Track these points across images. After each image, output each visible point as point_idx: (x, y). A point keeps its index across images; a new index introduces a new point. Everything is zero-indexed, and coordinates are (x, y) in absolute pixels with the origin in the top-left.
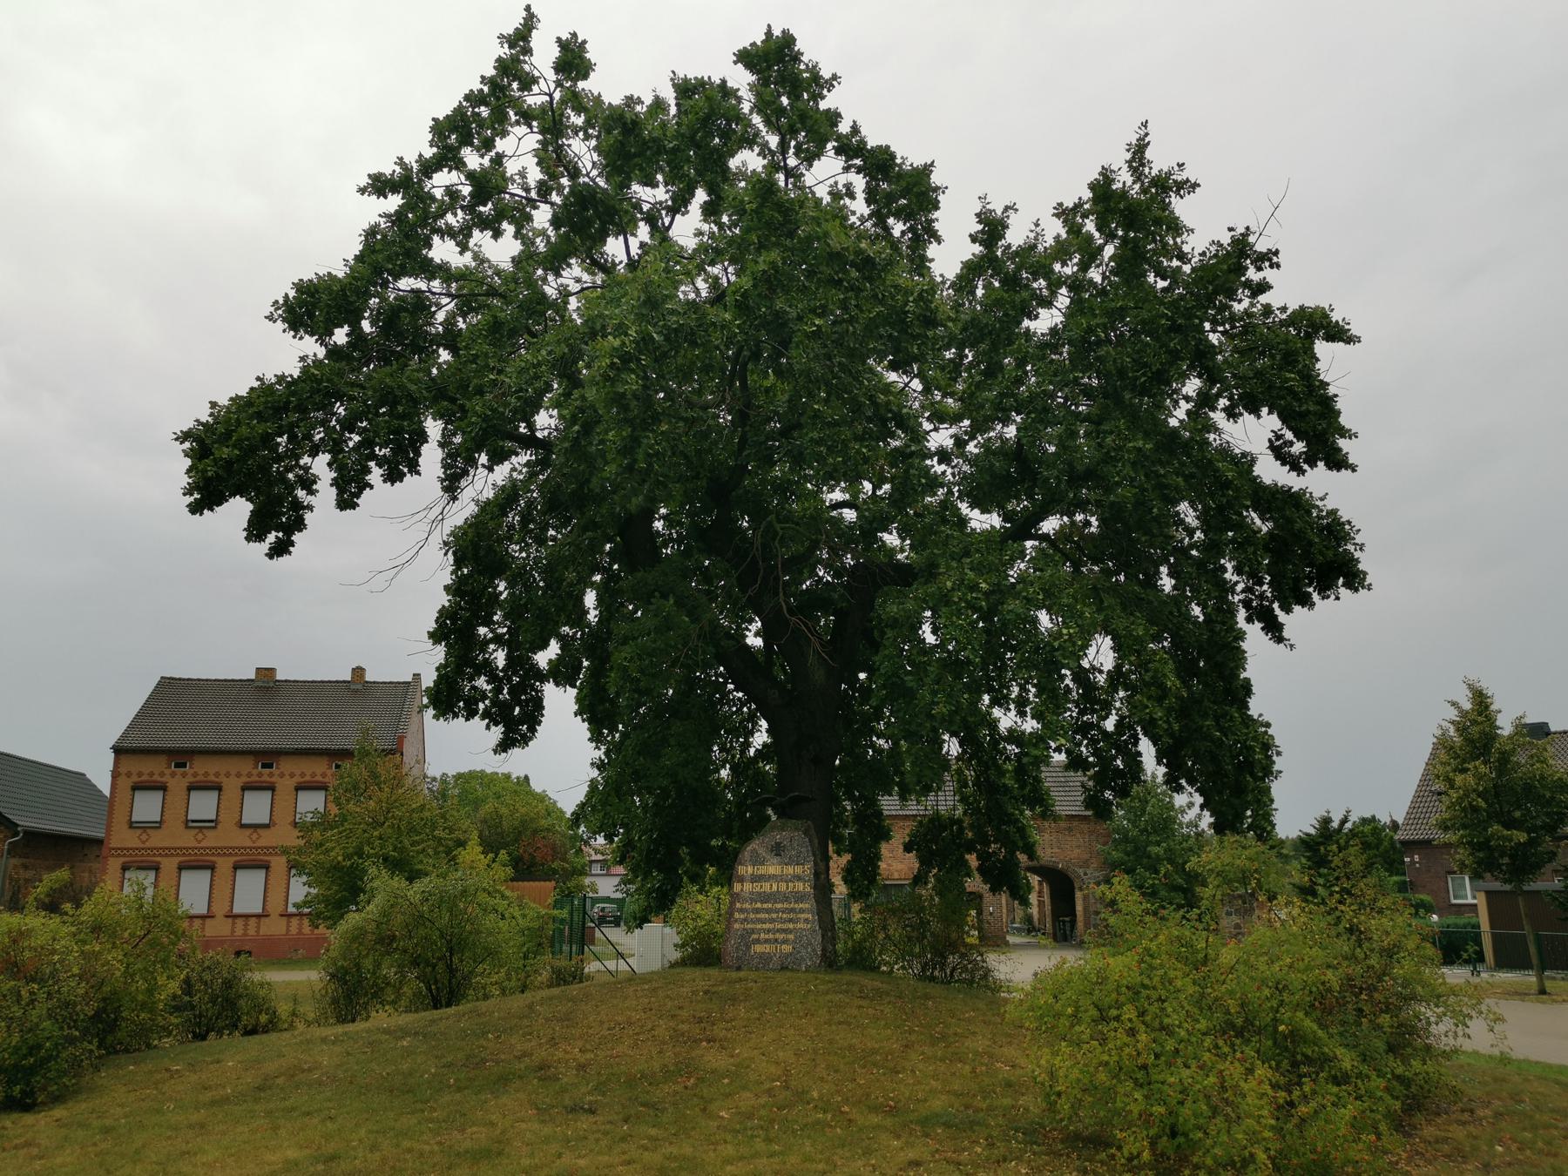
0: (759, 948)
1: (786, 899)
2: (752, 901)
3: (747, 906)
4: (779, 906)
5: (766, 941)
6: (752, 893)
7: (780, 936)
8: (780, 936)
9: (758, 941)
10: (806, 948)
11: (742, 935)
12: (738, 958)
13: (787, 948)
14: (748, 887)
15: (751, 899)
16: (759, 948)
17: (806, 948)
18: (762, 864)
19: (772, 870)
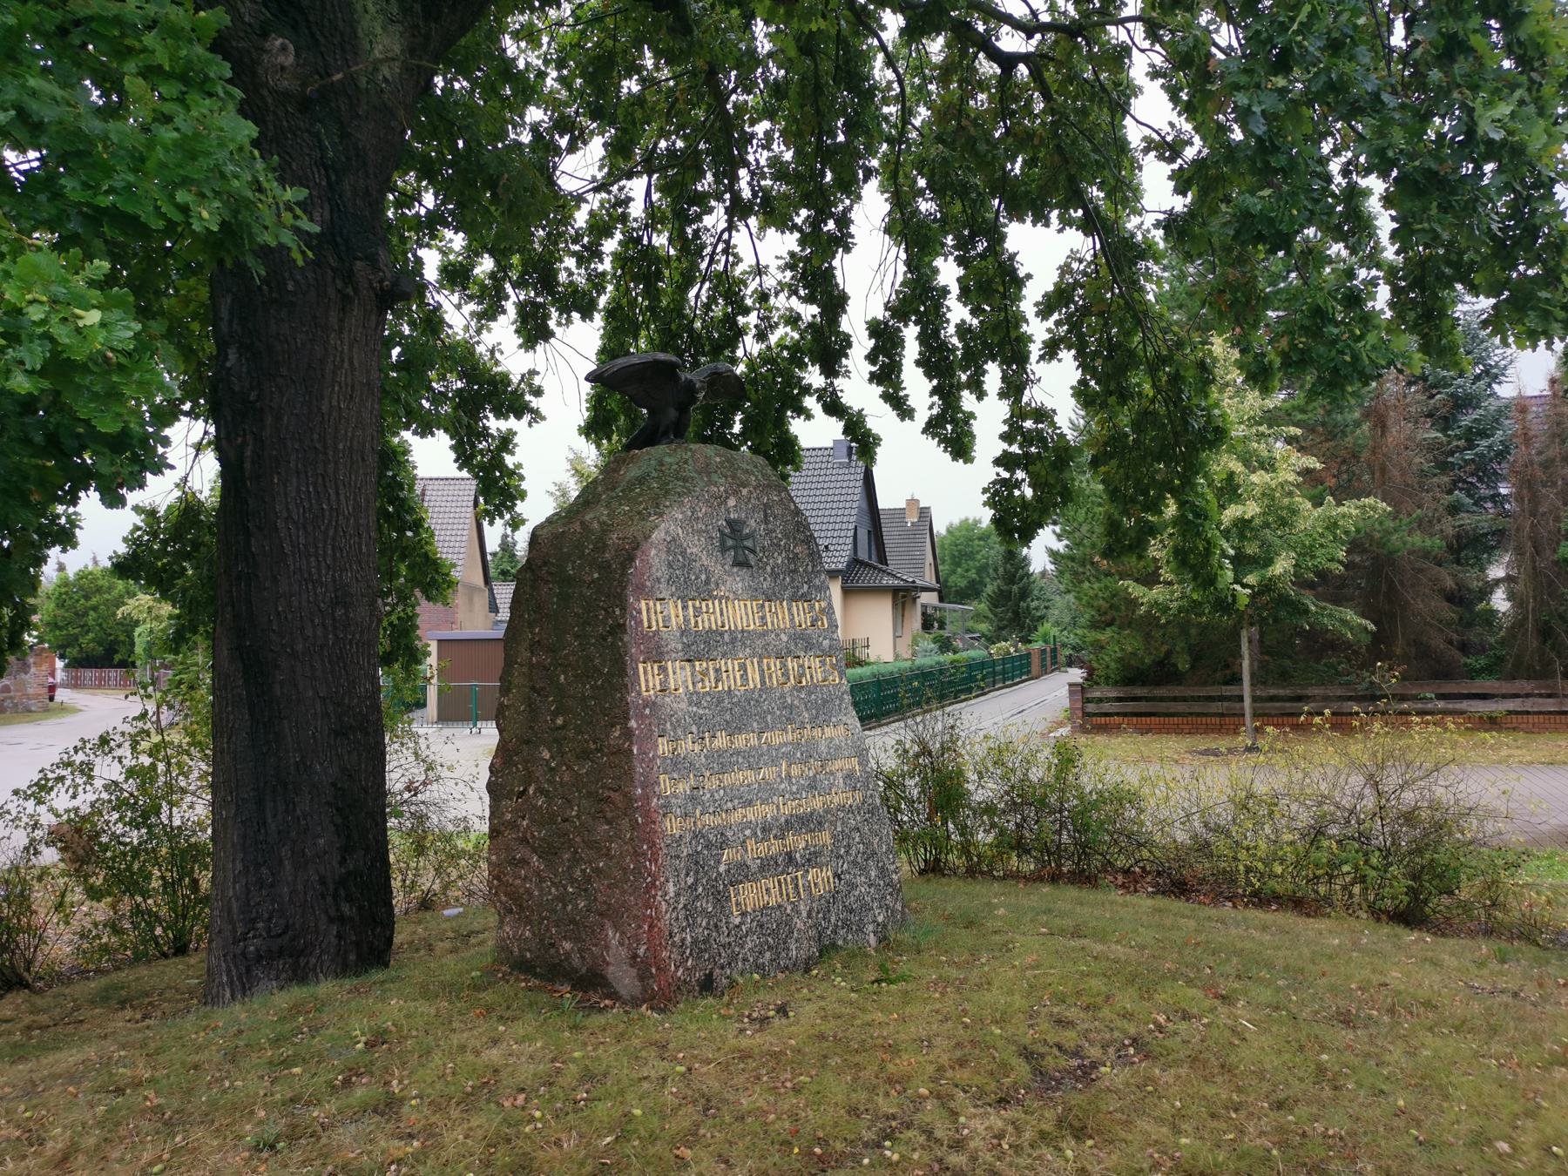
0: (749, 896)
1: (789, 716)
2: (705, 727)
3: (687, 746)
4: (776, 738)
5: (768, 866)
6: (695, 699)
7: (798, 842)
8: (798, 842)
9: (742, 874)
10: (864, 870)
11: (694, 857)
12: (700, 946)
13: (820, 878)
14: (679, 675)
15: (698, 720)
16: (749, 896)
17: (864, 870)
18: (706, 592)
19: (739, 614)
